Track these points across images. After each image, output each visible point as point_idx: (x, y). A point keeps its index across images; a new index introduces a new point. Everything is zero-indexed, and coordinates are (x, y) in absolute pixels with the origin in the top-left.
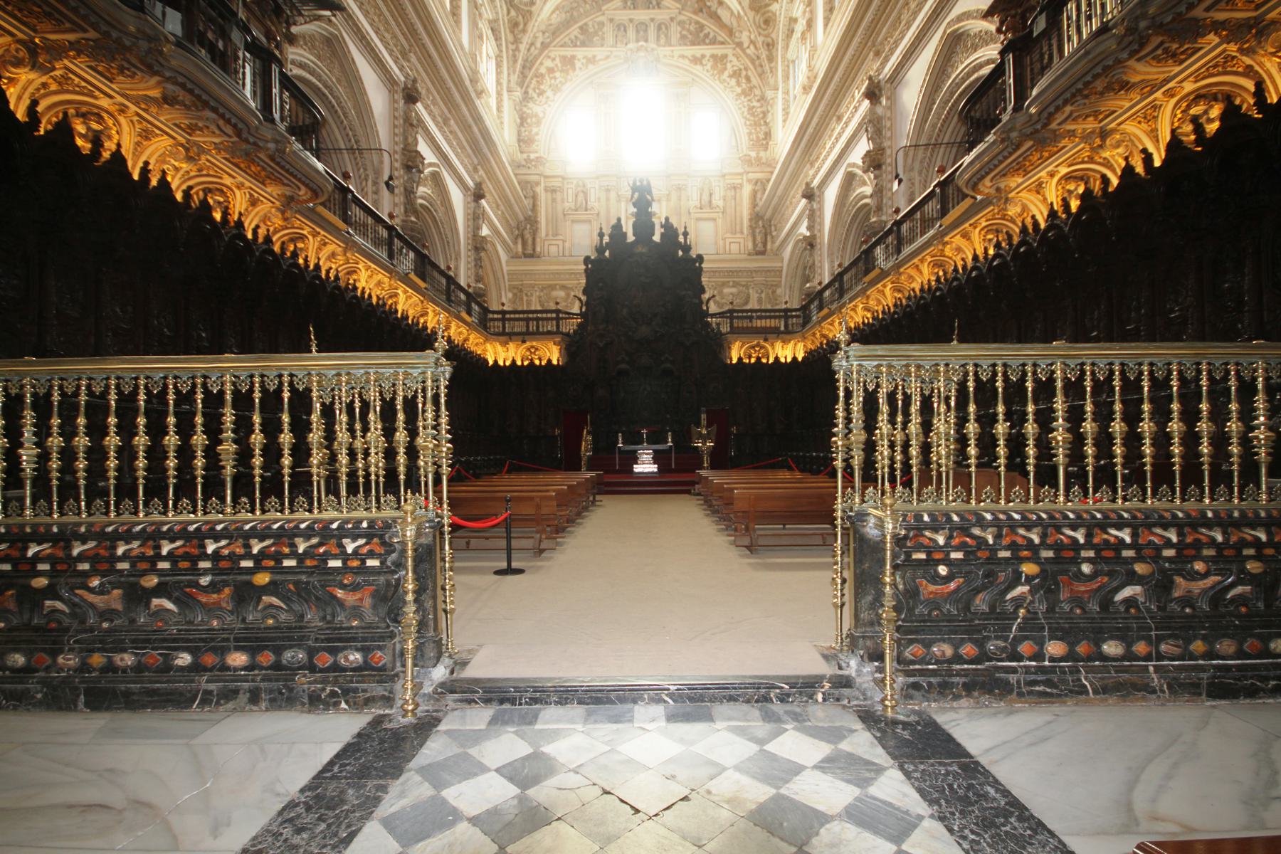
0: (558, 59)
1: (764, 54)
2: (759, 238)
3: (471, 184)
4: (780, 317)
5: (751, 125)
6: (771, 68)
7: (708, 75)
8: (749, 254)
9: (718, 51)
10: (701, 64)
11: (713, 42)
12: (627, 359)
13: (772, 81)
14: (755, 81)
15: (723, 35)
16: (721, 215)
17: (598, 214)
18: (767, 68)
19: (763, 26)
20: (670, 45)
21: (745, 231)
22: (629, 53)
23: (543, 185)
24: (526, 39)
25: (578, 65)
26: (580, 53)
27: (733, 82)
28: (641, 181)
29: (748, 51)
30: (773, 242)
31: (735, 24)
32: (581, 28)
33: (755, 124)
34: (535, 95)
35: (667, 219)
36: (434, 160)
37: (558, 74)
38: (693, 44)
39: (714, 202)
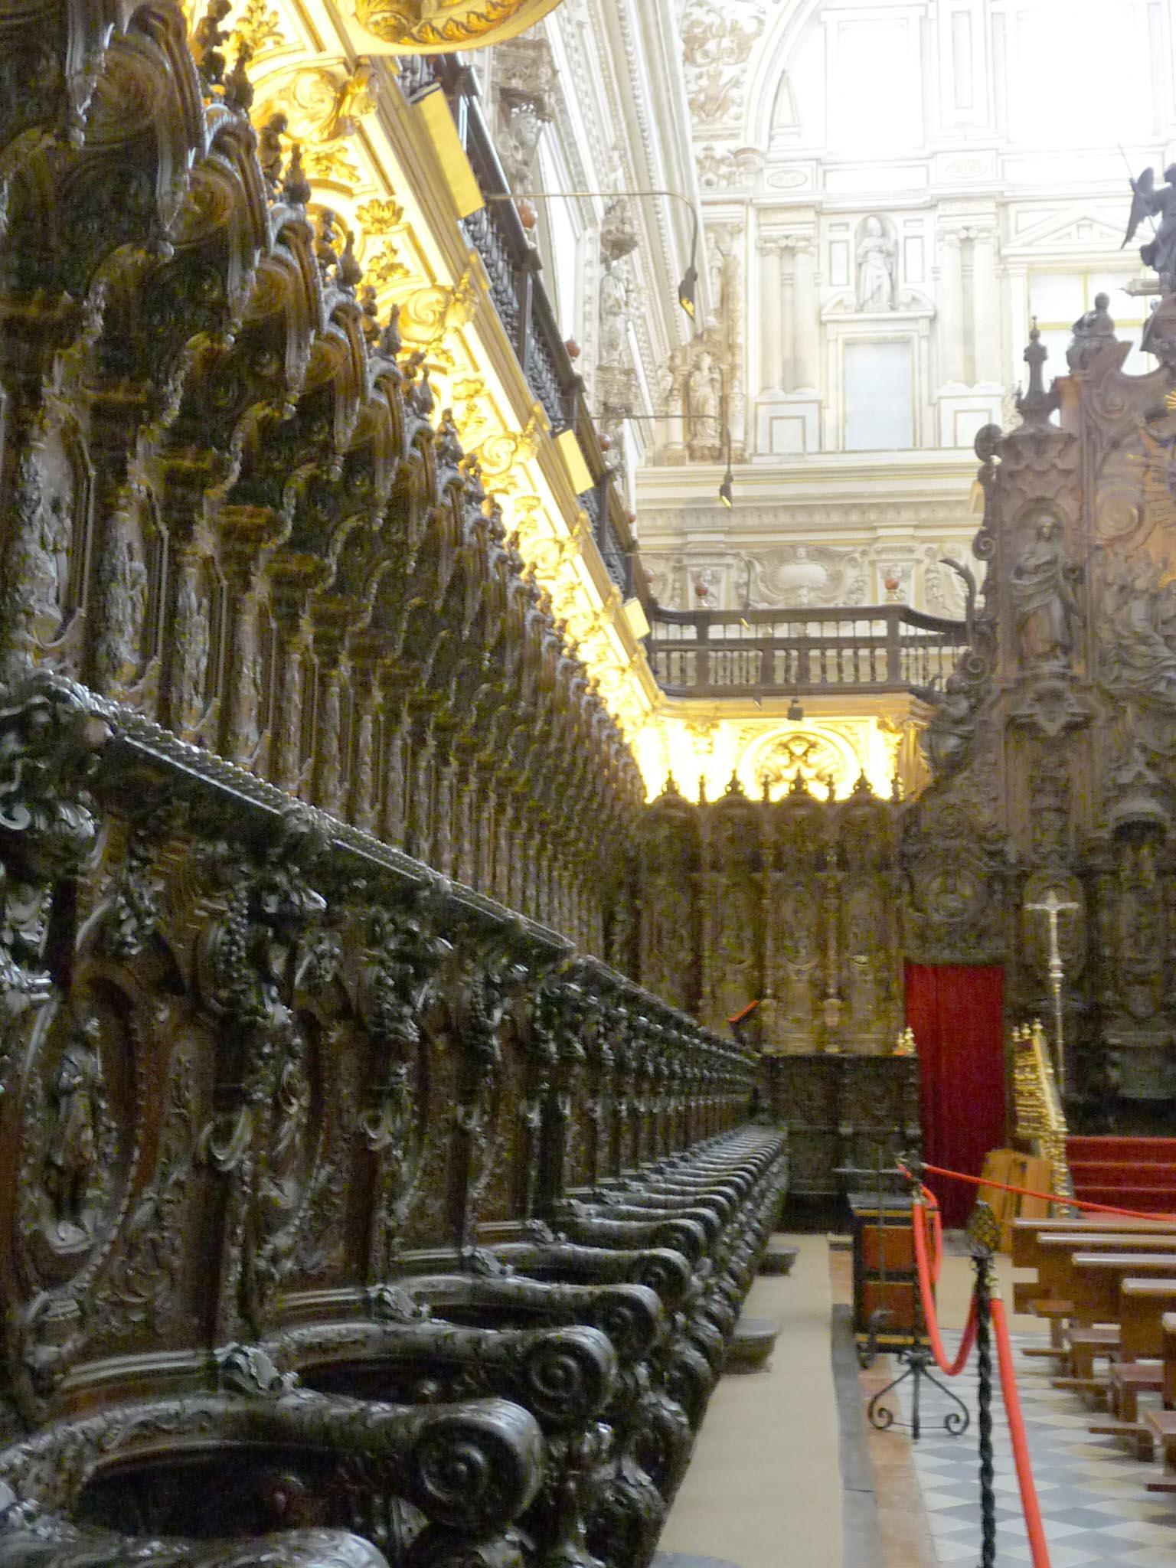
12: (1152, 777)
17: (933, 319)
23: (753, 232)
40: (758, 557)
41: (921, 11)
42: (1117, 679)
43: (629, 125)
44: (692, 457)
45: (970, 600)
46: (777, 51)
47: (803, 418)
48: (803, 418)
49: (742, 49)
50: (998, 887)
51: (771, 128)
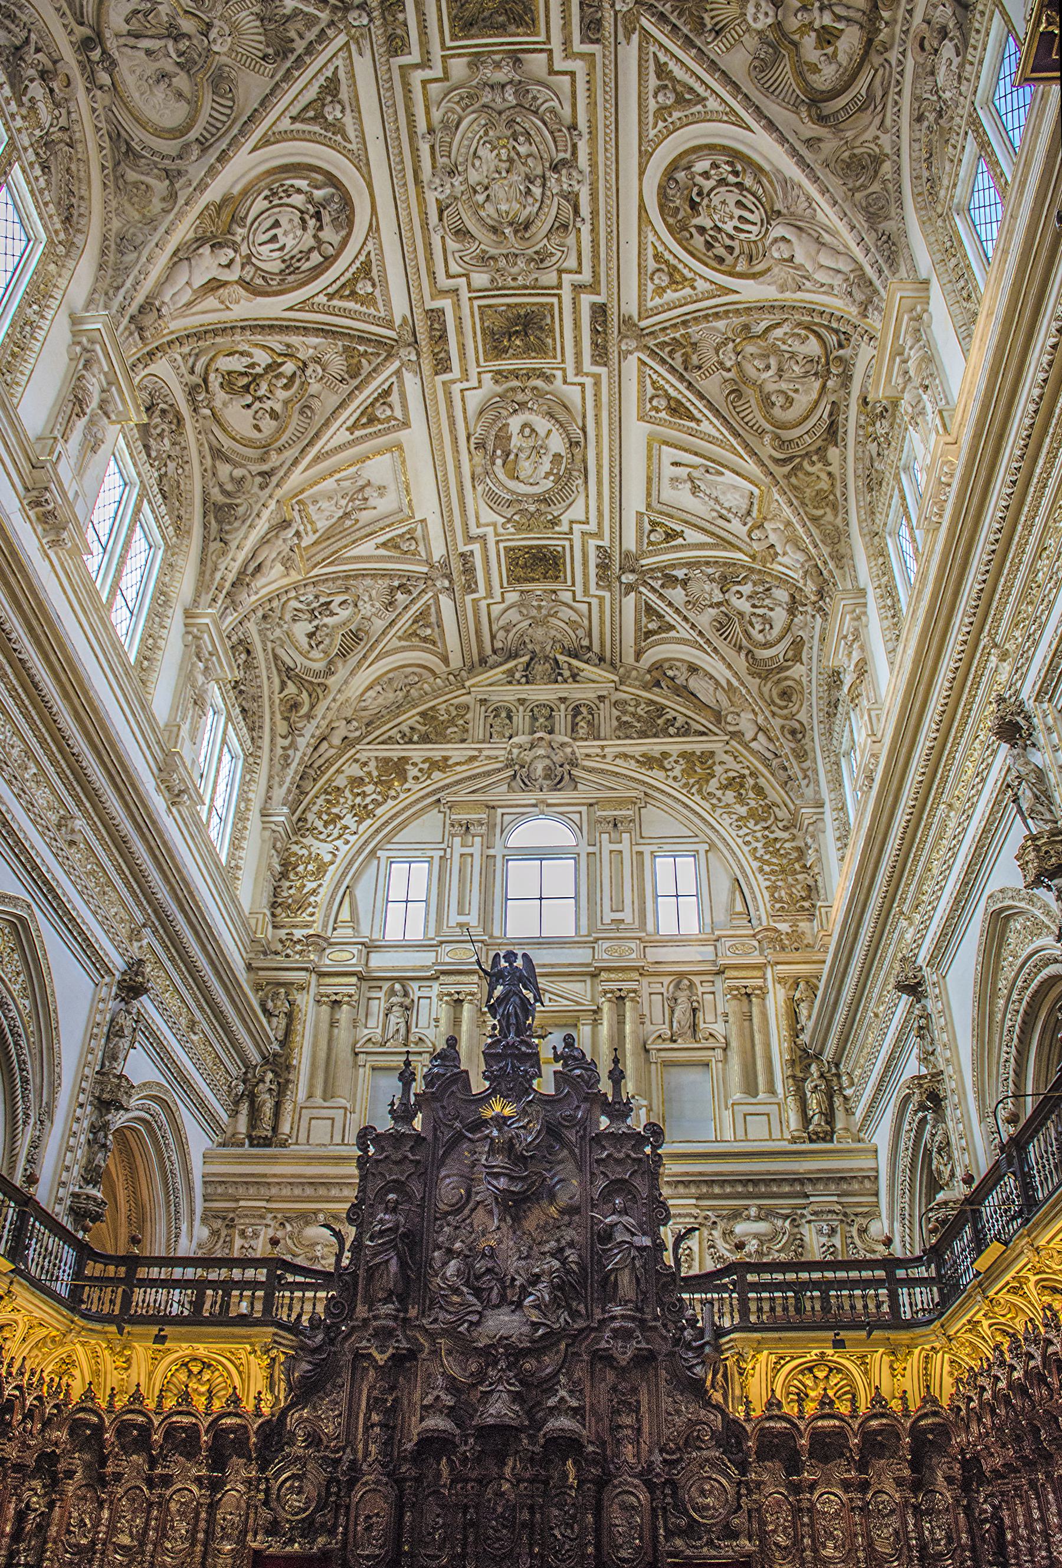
0: (373, 764)
1: (787, 747)
2: (813, 1103)
3: (118, 963)
4: (876, 1283)
5: (773, 872)
6: (804, 771)
7: (675, 785)
8: (794, 1140)
9: (696, 745)
10: (662, 767)
11: (685, 731)
12: (449, 1400)
13: (809, 792)
14: (775, 793)
15: (703, 721)
16: (719, 1051)
18: (795, 770)
19: (778, 701)
20: (599, 738)
21: (780, 1089)
22: (515, 751)
23: (313, 990)
24: (310, 731)
25: (413, 771)
26: (417, 753)
27: (730, 796)
28: (510, 956)
29: (753, 745)
30: (849, 1112)
31: (725, 703)
32: (423, 714)
33: (783, 871)
34: (319, 824)
35: (569, 1042)
36: (14, 889)
37: (369, 788)
38: (643, 734)
39: (702, 1026)
40: (288, 1219)
41: (442, 853)
42: (436, 1320)
43: (155, 911)
44: (251, 1145)
45: (339, 1257)
46: (344, 874)
47: (333, 1119)
48: (333, 1119)
49: (321, 870)
50: (334, 1490)
51: (335, 922)
